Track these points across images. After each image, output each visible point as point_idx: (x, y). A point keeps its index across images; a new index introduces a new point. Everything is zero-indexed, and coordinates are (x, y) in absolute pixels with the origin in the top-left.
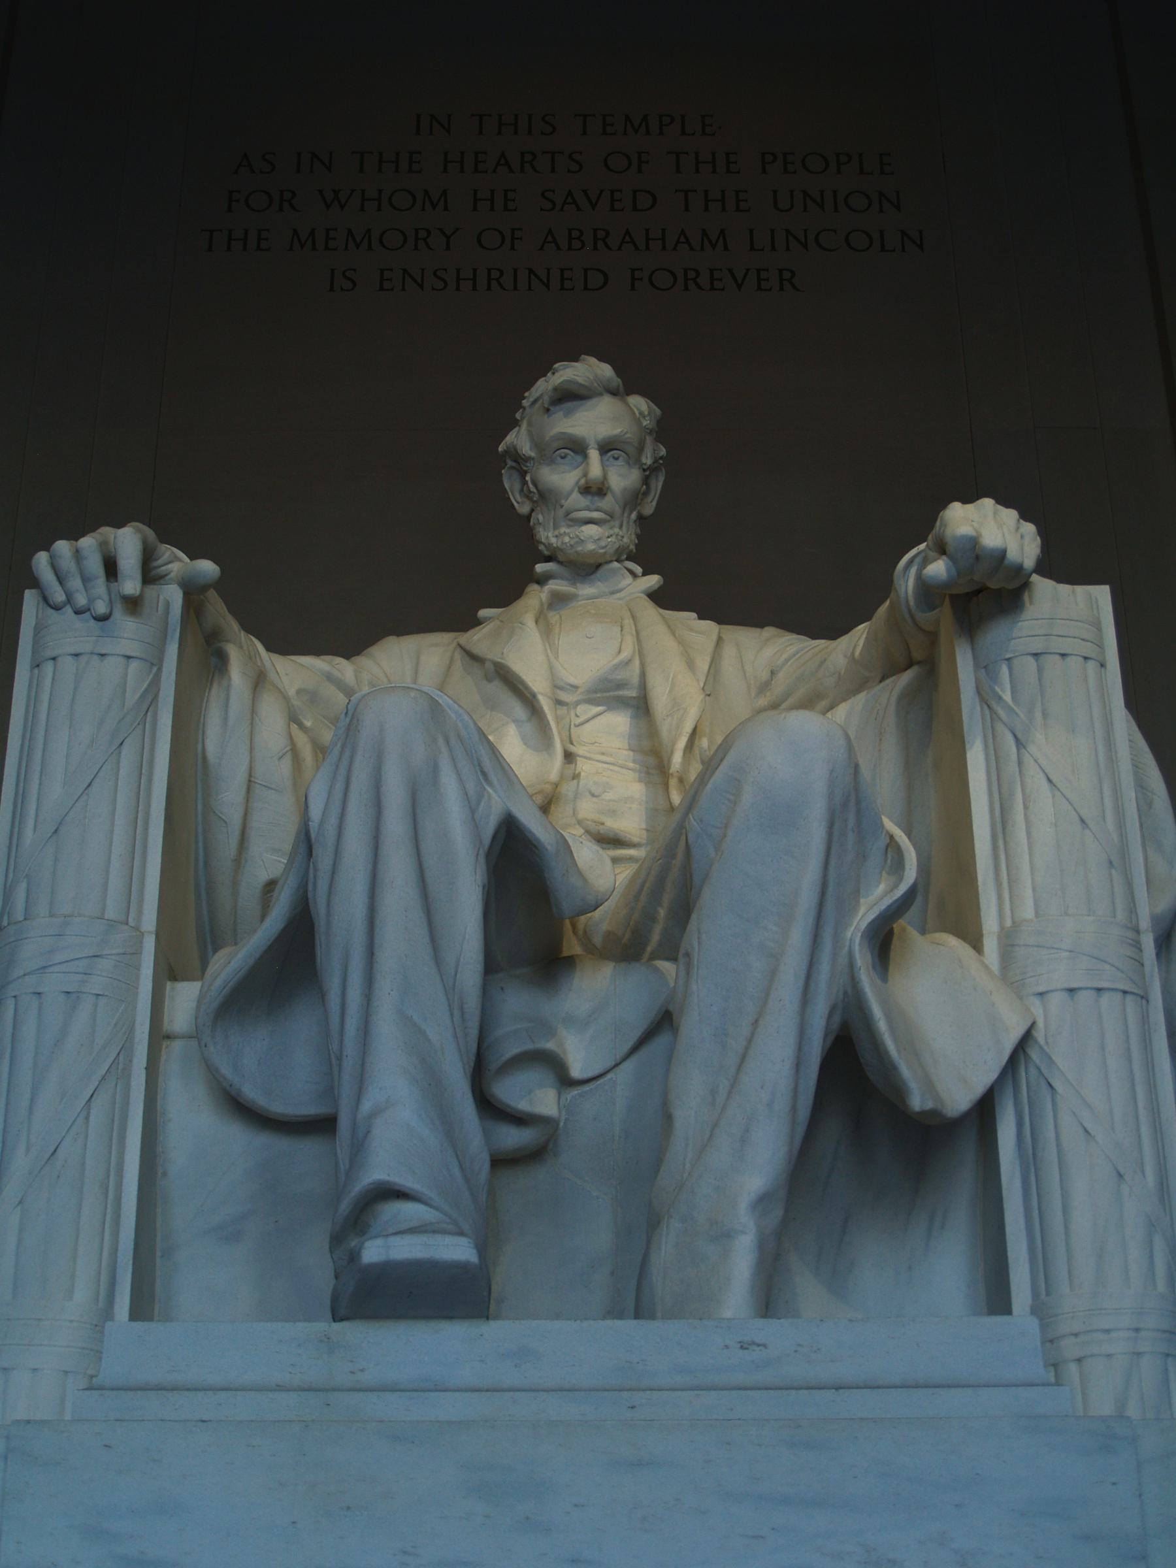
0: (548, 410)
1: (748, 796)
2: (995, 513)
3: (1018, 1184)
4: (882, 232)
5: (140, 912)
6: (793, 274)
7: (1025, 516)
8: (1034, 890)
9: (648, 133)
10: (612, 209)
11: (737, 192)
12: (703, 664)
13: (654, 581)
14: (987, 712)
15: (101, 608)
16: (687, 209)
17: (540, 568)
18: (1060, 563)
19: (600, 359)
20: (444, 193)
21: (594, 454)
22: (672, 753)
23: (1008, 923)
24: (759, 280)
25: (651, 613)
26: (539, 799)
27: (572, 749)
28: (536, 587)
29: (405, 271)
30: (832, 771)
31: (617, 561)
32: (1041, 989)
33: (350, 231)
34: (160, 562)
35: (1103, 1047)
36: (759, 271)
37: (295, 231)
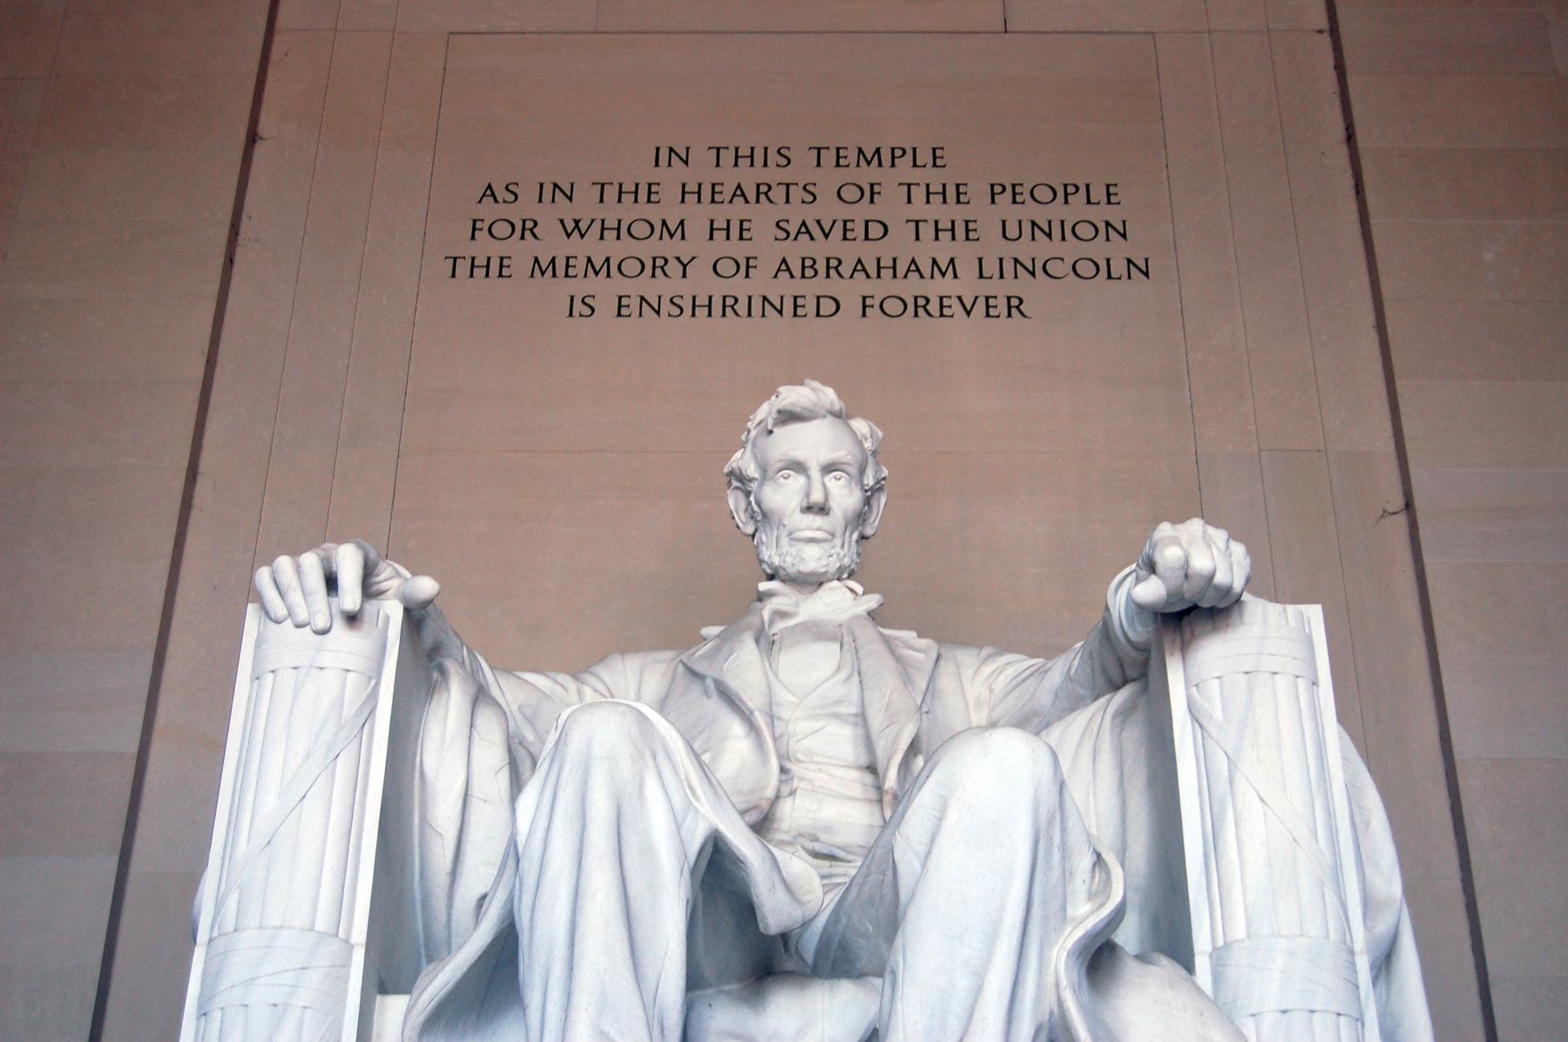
0: (771, 432)
1: (952, 816)
2: (1204, 533)
4: (1108, 261)
5: (350, 924)
6: (1021, 301)
7: (1234, 536)
8: (1246, 909)
9: (880, 165)
10: (845, 238)
11: (967, 222)
12: (922, 684)
13: (873, 601)
14: (1198, 730)
15: (321, 623)
16: (917, 238)
17: (764, 586)
18: (1273, 582)
19: (825, 383)
20: (682, 223)
21: (815, 473)
22: (886, 770)
23: (1220, 943)
24: (988, 307)
25: (868, 634)
26: (754, 817)
27: (788, 765)
28: (758, 604)
29: (642, 298)
32: (1254, 1011)
33: (589, 260)
34: (381, 578)
36: (987, 298)
37: (536, 260)
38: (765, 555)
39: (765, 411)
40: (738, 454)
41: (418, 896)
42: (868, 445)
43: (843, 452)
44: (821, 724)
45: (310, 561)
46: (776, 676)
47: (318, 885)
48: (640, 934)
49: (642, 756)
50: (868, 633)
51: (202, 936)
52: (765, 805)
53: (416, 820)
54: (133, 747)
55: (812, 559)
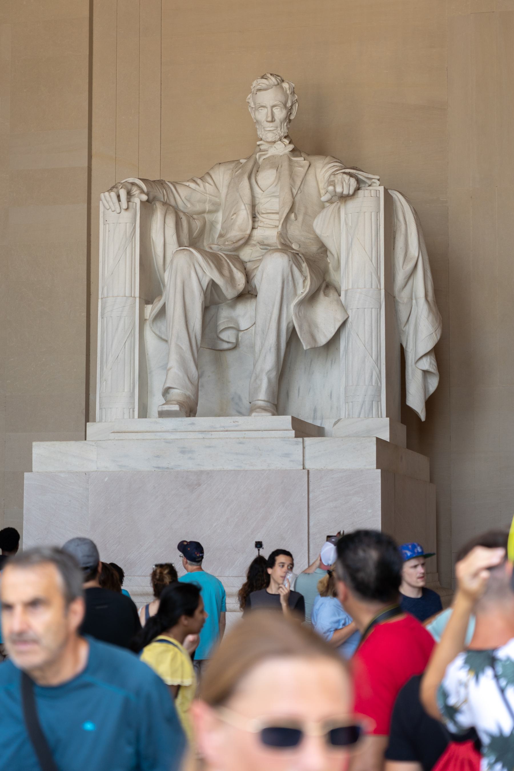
1: (264, 276)
2: (342, 178)
3: (344, 357)
12: (298, 183)
13: (291, 147)
15: (118, 212)
19: (271, 74)
21: (269, 109)
30: (283, 269)
31: (280, 140)
35: (364, 324)
38: (259, 133)
39: (254, 83)
40: (249, 96)
41: (157, 269)
42: (288, 92)
43: (276, 103)
44: (269, 199)
45: (113, 194)
46: (257, 183)
47: (125, 284)
48: (189, 315)
49: (190, 266)
50: (286, 164)
51: (100, 296)
52: (247, 236)
53: (153, 250)
54: (86, 165)
55: (270, 137)
